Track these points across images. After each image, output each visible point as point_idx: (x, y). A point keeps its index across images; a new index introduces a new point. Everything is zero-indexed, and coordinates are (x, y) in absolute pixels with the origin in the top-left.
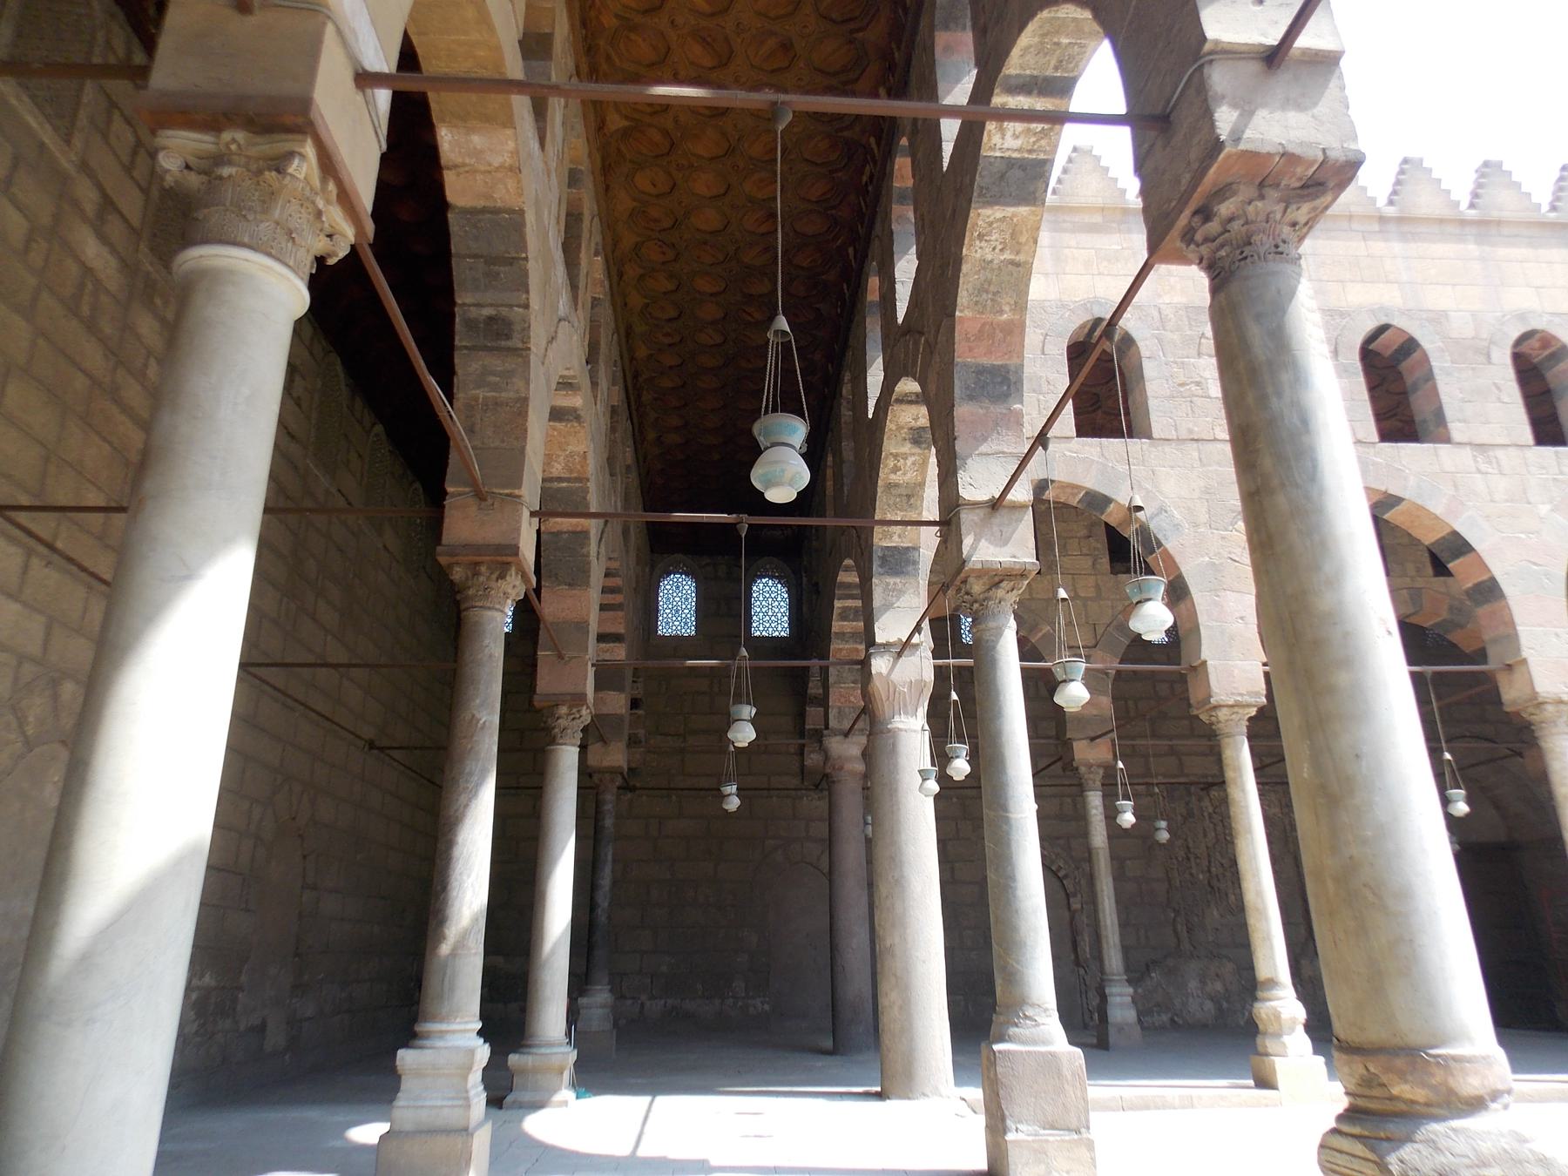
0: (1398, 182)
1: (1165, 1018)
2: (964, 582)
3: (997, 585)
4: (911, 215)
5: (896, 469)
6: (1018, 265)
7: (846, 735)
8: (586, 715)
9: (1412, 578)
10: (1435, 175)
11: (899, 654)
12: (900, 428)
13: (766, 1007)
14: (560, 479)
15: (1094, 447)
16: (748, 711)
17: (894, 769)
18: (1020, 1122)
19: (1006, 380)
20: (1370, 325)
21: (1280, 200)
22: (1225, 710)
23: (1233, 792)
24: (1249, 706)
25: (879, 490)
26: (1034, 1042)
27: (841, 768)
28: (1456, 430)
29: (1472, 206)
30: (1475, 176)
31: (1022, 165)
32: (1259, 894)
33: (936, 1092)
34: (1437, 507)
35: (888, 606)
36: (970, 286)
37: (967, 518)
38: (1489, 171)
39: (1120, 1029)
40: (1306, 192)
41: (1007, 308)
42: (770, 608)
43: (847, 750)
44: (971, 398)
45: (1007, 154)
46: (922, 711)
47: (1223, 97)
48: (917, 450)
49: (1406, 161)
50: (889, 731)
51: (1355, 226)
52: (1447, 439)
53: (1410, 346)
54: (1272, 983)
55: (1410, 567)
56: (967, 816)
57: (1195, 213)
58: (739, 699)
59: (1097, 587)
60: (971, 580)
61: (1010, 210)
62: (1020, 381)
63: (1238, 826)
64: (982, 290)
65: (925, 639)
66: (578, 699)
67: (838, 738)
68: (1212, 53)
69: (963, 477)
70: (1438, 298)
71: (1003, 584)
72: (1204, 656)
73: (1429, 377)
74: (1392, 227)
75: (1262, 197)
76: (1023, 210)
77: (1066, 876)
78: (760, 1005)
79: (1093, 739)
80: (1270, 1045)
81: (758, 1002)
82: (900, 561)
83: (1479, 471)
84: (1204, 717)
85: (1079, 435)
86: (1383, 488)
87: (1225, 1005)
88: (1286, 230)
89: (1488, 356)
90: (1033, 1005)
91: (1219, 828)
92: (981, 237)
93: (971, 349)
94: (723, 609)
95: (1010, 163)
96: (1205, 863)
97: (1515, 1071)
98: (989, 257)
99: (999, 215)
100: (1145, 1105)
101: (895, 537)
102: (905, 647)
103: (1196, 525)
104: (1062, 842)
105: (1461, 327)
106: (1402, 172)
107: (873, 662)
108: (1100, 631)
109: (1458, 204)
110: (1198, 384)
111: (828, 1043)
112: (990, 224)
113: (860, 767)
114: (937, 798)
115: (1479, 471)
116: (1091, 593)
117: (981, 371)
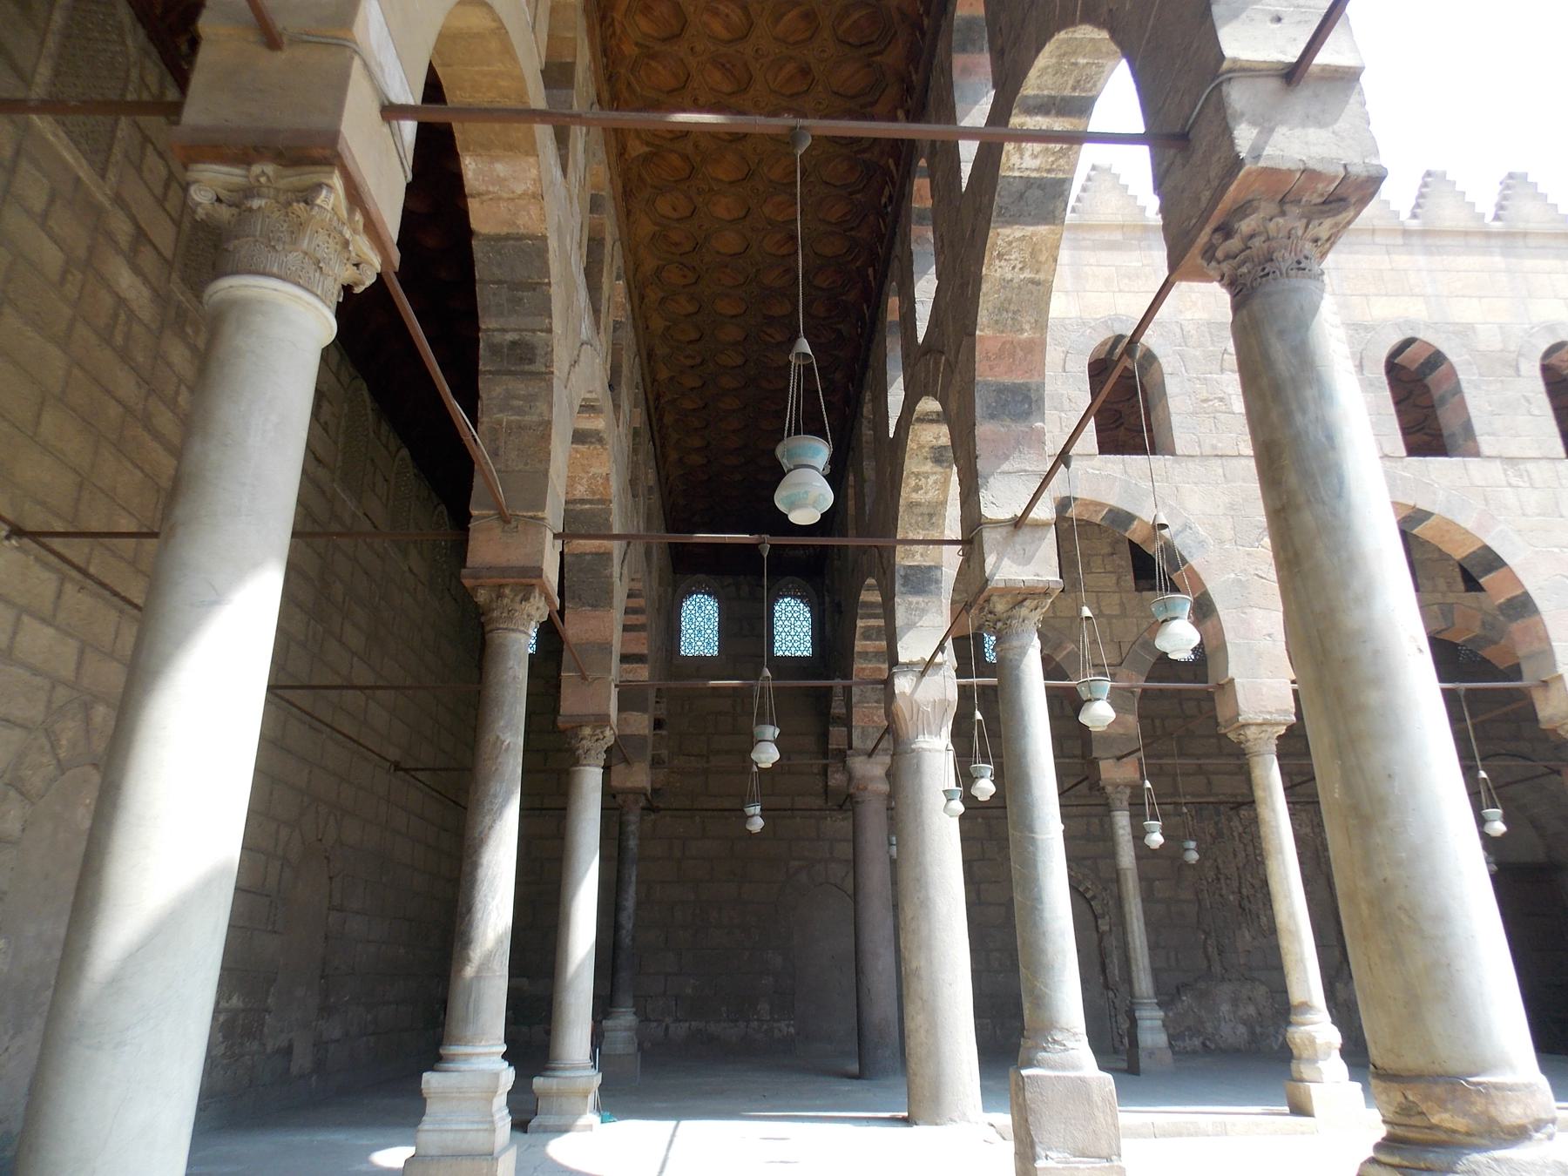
0: (1421, 195)
1: (1197, 1042)
2: (988, 601)
4: (930, 235)
5: (917, 488)
6: (1038, 283)
7: (870, 755)
8: (609, 736)
9: (1444, 594)
10: (1459, 188)
11: (923, 674)
12: (921, 447)
13: (792, 1030)
14: (583, 501)
15: (1116, 464)
16: (772, 732)
17: (918, 790)
18: (1050, 1149)
19: (1027, 398)
20: (1396, 339)
21: (1302, 216)
22: (1253, 729)
23: (1263, 812)
24: (1278, 724)
25: (901, 509)
26: (1064, 1068)
27: (865, 789)
28: (1485, 443)
29: (1497, 218)
30: (1500, 187)
31: (1040, 184)
32: (1292, 915)
33: (964, 1117)
34: (1468, 521)
35: (911, 626)
37: (989, 537)
38: (1513, 183)
39: (1151, 1054)
40: (1326, 208)
41: (1027, 327)
42: (792, 628)
43: (870, 770)
44: (992, 417)
45: (1025, 174)
47: (1242, 115)
48: (939, 469)
49: (1429, 174)
51: (1378, 239)
52: (1476, 453)
53: (1436, 359)
54: (1306, 1007)
55: (1441, 583)
56: (992, 836)
57: (1216, 230)
59: (1122, 604)
60: (994, 598)
61: (1030, 229)
62: (1041, 399)
63: (1269, 846)
64: (1002, 309)
65: (949, 658)
66: (602, 720)
68: (1230, 71)
69: (985, 496)
70: (1465, 311)
71: (1027, 603)
72: (1231, 674)
73: (1457, 390)
74: (1415, 240)
75: (1283, 214)
76: (1043, 229)
77: (1094, 897)
78: (785, 1028)
79: (1119, 758)
80: (1306, 1071)
81: (783, 1025)
82: (922, 580)
83: (1510, 485)
84: (1230, 735)
85: (1101, 453)
86: (1411, 503)
87: (1258, 1030)
88: (1308, 246)
89: (1517, 369)
90: (1062, 1030)
91: (1250, 849)
92: (1000, 256)
94: (746, 630)
95: (1029, 183)
96: (1235, 884)
97: (1558, 1098)
98: (1009, 276)
99: (1018, 234)
100: (1178, 1133)
101: (918, 557)
102: (928, 666)
103: (1222, 542)
104: (1089, 862)
105: (1488, 339)
106: (1425, 185)
108: (1125, 650)
109: (1483, 216)
110: (1221, 400)
111: (854, 1067)
112: (1010, 243)
113: (884, 787)
114: (962, 818)
115: (1510, 485)
116: (1116, 611)
117: (1002, 389)
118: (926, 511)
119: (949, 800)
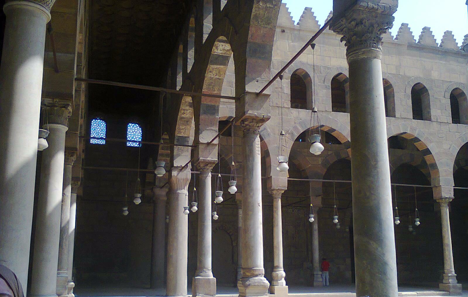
2: (199, 163)
3: (207, 165)
4: (194, 35)
5: (184, 113)
6: (220, 79)
7: (162, 187)
11: (181, 170)
12: (186, 102)
16: (139, 195)
17: (177, 205)
18: (200, 293)
19: (215, 109)
20: (336, 73)
22: (275, 191)
23: (275, 214)
24: (282, 190)
25: (178, 119)
31: (222, 56)
32: (278, 243)
33: (182, 295)
35: (178, 155)
36: (206, 84)
37: (201, 147)
41: (216, 90)
42: (134, 133)
43: (161, 193)
44: (204, 113)
46: (187, 188)
50: (176, 193)
56: (195, 221)
57: (242, 121)
58: (137, 193)
60: (201, 163)
62: (218, 110)
63: (275, 224)
64: (209, 85)
65: (190, 165)
67: (158, 189)
68: (246, 93)
69: (201, 136)
71: (209, 165)
72: (271, 175)
82: (183, 141)
84: (270, 192)
86: (330, 126)
88: (257, 128)
90: (205, 268)
92: (210, 72)
93: (206, 100)
94: (116, 132)
98: (212, 77)
99: (215, 67)
101: (182, 133)
102: (182, 169)
107: (173, 172)
112: (213, 69)
113: (165, 199)
114: (189, 214)
118: (186, 120)
119: (185, 210)
